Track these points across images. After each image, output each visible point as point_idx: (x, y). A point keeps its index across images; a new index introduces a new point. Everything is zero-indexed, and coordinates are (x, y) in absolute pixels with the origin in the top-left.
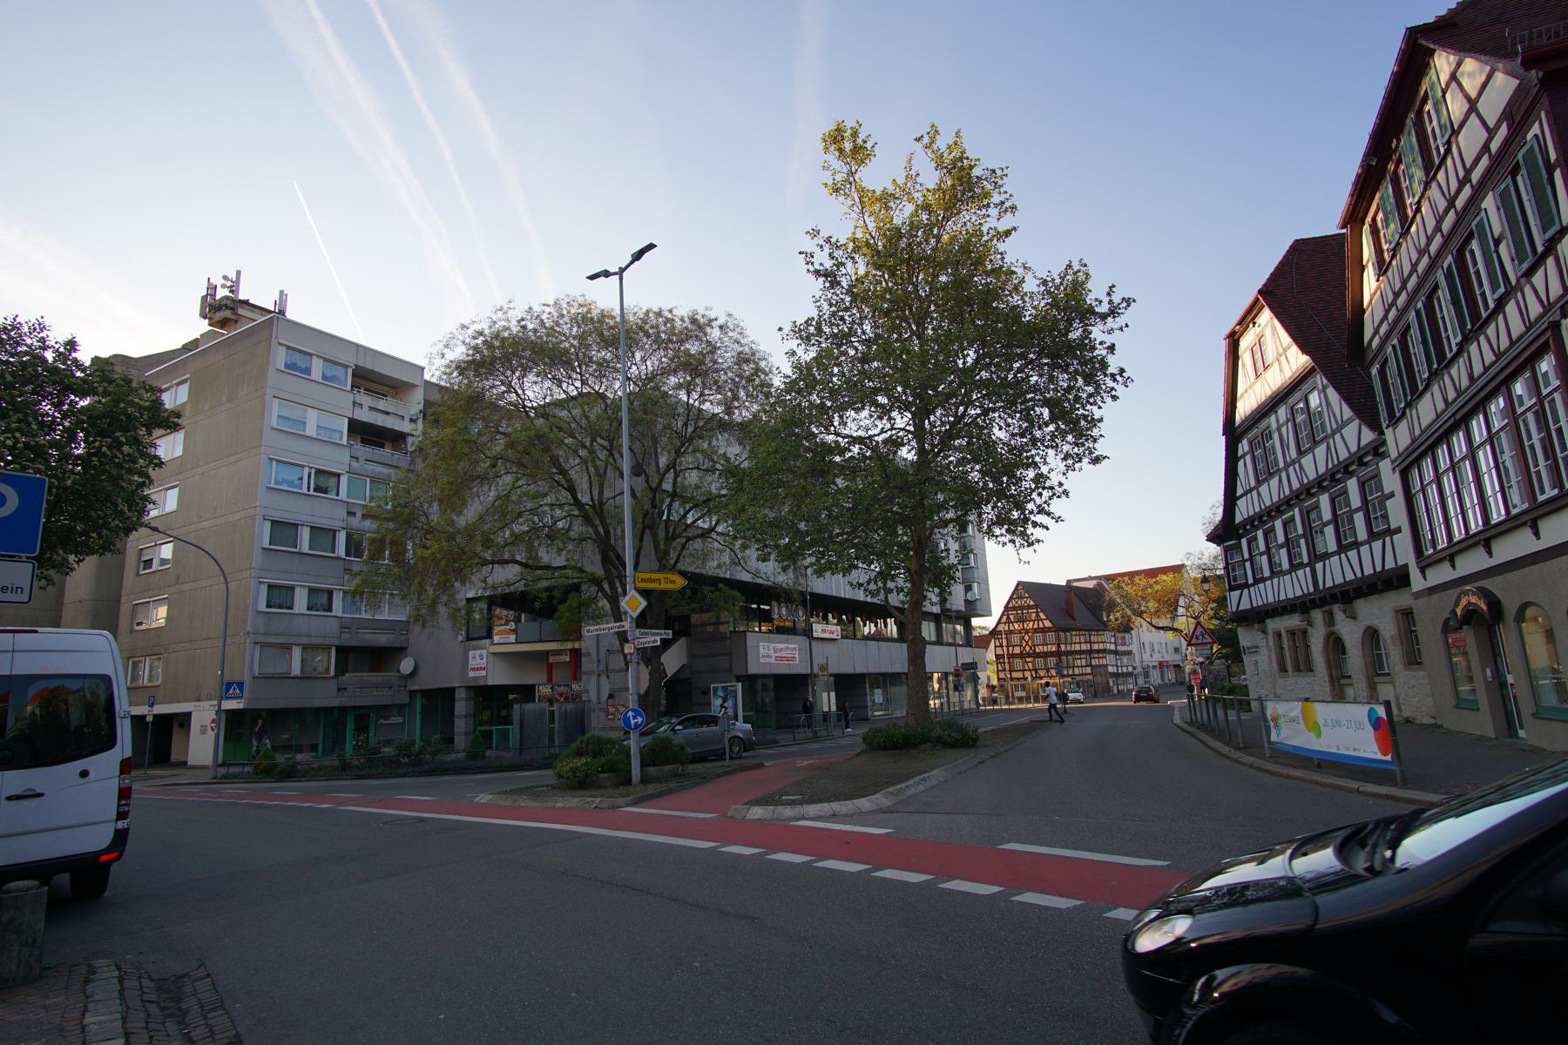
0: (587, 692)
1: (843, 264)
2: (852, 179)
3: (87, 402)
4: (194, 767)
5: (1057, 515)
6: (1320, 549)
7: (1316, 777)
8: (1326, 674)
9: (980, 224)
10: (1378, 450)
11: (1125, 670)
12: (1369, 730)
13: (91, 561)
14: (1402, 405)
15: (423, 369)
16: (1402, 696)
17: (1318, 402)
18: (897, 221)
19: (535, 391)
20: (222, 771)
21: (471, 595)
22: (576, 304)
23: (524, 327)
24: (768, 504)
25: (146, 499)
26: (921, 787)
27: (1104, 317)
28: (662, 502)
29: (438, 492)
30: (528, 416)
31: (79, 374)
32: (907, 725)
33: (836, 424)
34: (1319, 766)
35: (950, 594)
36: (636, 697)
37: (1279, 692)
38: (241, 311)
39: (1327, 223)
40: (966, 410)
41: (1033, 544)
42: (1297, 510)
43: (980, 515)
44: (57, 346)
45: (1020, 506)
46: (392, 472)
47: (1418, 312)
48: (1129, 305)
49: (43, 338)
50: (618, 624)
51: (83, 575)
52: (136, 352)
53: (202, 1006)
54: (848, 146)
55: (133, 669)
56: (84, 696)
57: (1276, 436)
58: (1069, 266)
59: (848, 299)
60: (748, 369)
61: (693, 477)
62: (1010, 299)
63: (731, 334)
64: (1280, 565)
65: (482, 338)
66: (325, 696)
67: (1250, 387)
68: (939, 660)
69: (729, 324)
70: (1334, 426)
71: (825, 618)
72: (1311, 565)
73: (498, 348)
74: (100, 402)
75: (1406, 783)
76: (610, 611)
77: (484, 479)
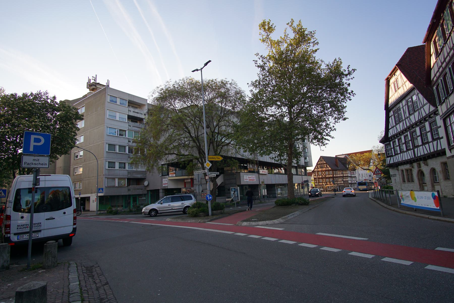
0: (196, 190)
1: (266, 63)
2: (268, 37)
3: (59, 113)
4: (91, 211)
5: (332, 136)
6: (416, 144)
7: (414, 214)
8: (418, 182)
9: (307, 48)
10: (435, 113)
11: (354, 182)
12: (432, 200)
13: (63, 156)
14: (444, 98)
15: (147, 100)
16: (443, 189)
17: (416, 98)
18: (282, 49)
19: (178, 105)
20: (99, 212)
21: (163, 163)
22: (188, 79)
23: (174, 87)
24: (246, 135)
25: (76, 139)
26: (292, 217)
27: (346, 75)
28: (215, 135)
29: (153, 135)
30: (176, 112)
31: (57, 106)
32: (288, 199)
33: (265, 111)
34: (416, 210)
35: (300, 160)
36: (210, 191)
37: (403, 188)
38: (97, 86)
39: (419, 41)
40: (304, 105)
41: (325, 145)
42: (408, 132)
43: (309, 137)
44: (51, 98)
45: (321, 134)
46: (140, 129)
47: (449, 69)
48: (354, 71)
49: (47, 96)
50: (204, 171)
51: (60, 160)
52: (71, 99)
53: (98, 274)
54: (267, 27)
55: (75, 185)
56: (63, 192)
57: (402, 110)
58: (335, 60)
59: (268, 74)
60: (238, 96)
61: (224, 128)
62: (317, 71)
63: (233, 85)
64: (403, 149)
65: (163, 91)
66: (124, 192)
67: (393, 95)
68: (297, 180)
69: (232, 83)
70: (421, 106)
71: (263, 168)
72: (413, 149)
73: (167, 93)
74: (62, 113)
75: (444, 216)
76: (201, 167)
77: (165, 130)
